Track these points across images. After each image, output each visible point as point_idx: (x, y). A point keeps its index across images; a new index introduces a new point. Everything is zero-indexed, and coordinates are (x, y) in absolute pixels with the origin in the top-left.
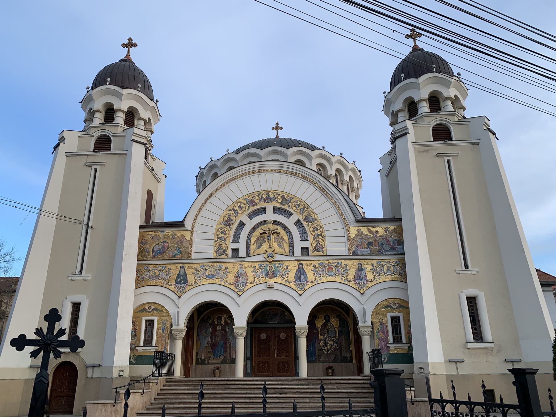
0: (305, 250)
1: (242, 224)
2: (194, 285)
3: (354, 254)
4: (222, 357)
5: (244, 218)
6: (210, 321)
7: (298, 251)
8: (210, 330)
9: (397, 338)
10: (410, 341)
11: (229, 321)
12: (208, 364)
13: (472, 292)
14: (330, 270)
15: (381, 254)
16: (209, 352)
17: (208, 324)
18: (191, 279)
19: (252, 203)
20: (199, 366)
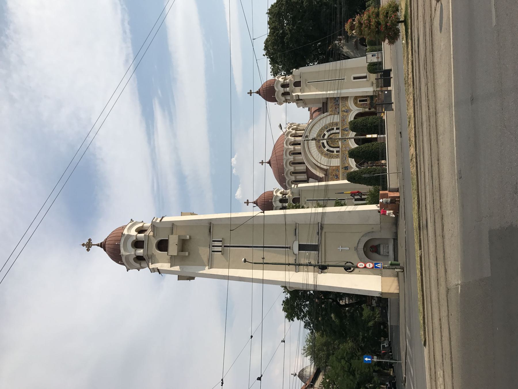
0: (337, 129)
1: (328, 150)
2: (349, 164)
3: (339, 113)
5: (325, 149)
7: (338, 131)
9: (366, 100)
10: (367, 96)
13: (352, 78)
14: (344, 120)
15: (339, 105)
18: (347, 165)
19: (320, 147)
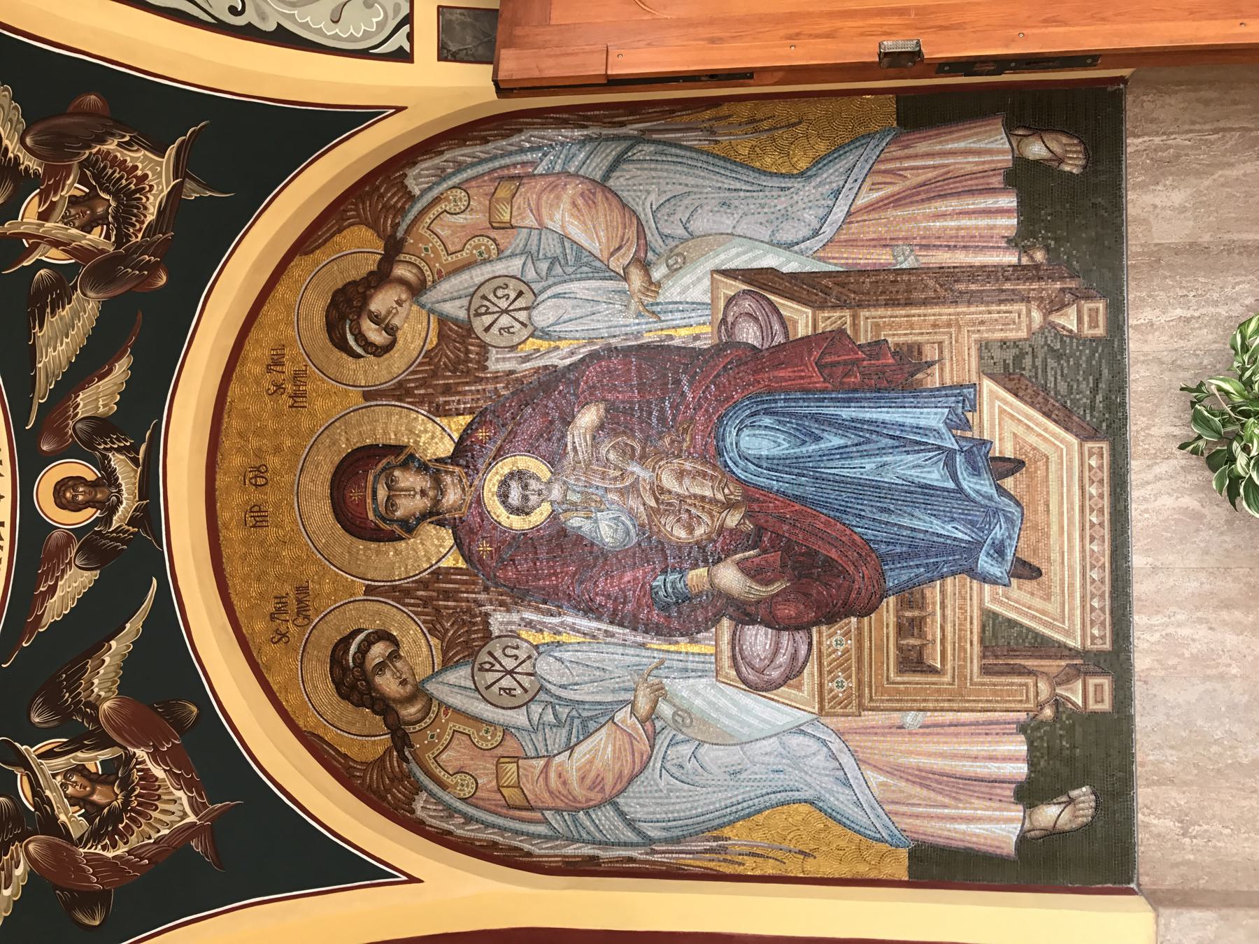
4: (1006, 420)
6: (419, 647)
8: (572, 652)
11: (416, 333)
12: (1115, 661)
16: (913, 662)
17: (454, 687)
20: (1155, 817)
